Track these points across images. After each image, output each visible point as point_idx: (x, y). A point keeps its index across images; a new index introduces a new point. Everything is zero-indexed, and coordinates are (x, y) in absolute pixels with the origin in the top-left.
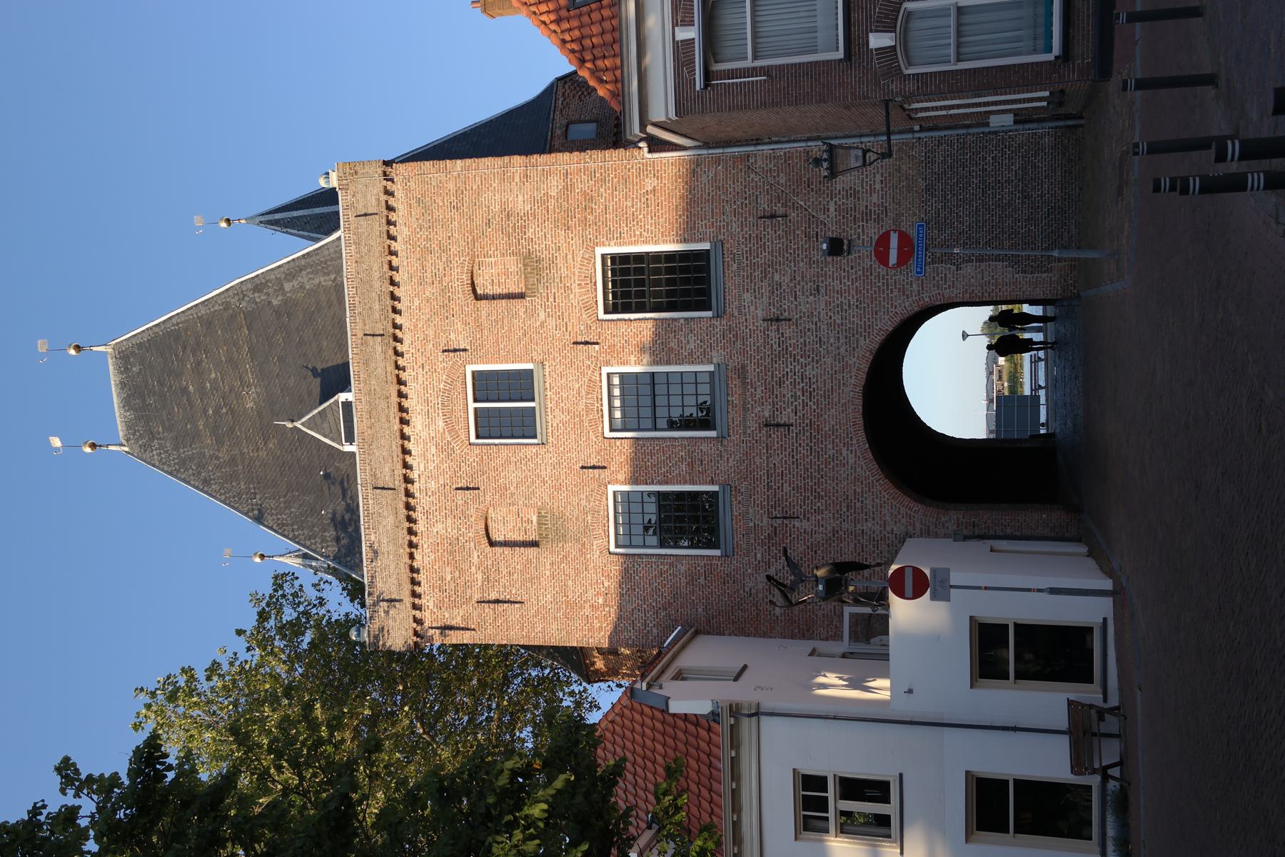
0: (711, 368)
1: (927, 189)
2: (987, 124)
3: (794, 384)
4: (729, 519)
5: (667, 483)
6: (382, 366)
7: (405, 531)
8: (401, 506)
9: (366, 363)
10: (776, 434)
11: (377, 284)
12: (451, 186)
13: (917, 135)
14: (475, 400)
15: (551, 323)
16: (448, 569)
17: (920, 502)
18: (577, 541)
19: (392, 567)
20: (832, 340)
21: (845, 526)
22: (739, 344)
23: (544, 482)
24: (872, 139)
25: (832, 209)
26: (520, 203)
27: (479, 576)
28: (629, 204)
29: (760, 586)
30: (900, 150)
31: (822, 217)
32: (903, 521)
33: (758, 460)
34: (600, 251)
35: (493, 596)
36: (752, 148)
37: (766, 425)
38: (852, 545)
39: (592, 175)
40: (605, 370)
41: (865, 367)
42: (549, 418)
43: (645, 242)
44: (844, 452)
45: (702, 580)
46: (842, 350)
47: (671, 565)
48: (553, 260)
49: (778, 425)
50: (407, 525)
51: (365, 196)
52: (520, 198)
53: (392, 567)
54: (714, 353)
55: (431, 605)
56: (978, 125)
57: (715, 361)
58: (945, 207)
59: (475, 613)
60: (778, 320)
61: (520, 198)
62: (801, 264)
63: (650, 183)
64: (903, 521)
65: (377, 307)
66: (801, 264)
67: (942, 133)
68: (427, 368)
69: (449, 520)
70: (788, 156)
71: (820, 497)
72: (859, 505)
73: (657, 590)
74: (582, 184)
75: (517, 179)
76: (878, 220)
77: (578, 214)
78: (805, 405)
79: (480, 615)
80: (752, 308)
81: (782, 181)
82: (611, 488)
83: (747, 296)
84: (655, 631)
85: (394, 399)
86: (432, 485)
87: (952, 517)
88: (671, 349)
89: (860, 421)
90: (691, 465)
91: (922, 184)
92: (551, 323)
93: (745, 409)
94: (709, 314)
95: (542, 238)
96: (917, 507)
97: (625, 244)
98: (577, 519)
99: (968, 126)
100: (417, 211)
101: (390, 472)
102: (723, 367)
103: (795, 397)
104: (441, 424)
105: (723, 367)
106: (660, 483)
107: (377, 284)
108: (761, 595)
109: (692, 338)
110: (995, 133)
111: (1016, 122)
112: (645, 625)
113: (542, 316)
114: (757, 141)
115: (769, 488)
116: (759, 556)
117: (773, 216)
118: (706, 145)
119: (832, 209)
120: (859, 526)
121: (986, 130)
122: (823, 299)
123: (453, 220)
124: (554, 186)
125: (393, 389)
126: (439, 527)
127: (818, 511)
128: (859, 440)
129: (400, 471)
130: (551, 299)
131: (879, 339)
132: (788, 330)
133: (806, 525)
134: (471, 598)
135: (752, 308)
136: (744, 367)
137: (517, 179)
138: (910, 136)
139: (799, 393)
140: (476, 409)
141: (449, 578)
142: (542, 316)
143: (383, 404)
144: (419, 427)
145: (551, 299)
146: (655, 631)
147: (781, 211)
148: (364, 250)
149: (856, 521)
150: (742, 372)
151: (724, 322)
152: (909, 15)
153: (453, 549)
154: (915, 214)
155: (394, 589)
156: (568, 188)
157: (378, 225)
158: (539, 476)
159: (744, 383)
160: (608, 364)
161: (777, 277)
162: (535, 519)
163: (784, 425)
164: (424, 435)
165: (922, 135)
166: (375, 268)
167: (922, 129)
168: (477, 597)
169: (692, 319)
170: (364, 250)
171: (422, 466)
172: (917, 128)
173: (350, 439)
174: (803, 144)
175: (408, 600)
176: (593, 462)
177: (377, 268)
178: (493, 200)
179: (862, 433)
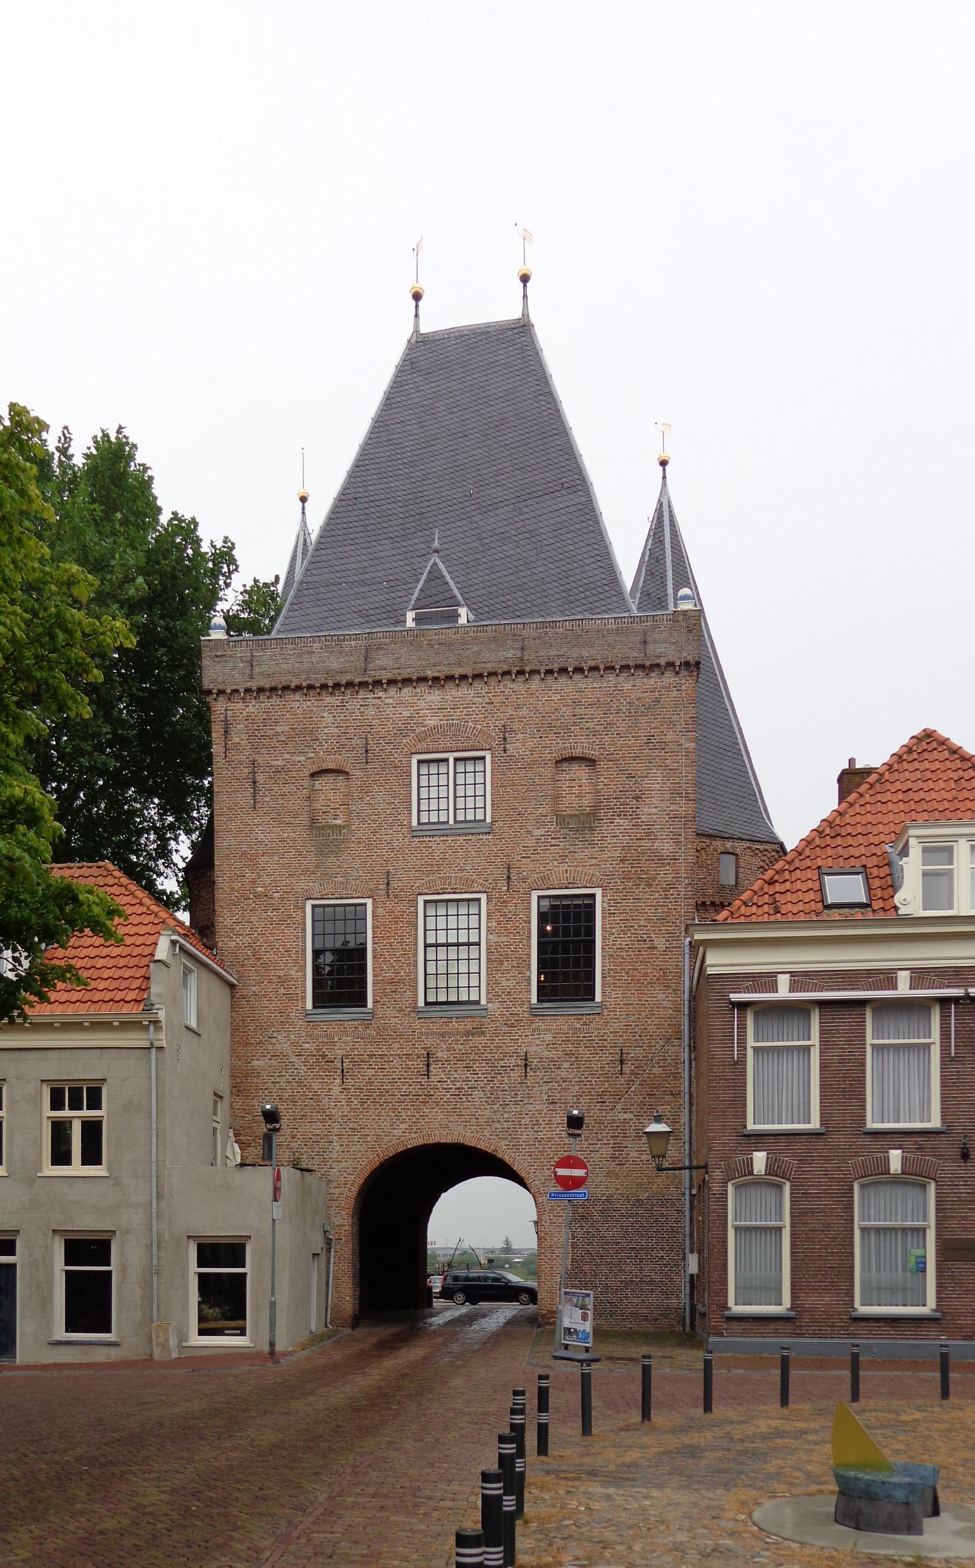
0: (483, 1002)
1: (638, 1201)
2: (692, 1252)
3: (467, 1080)
4: (342, 1017)
5: (374, 957)
6: (492, 658)
7: (323, 681)
8: (349, 677)
9: (495, 640)
10: (420, 1064)
11: (574, 653)
12: (670, 737)
13: (687, 1192)
14: (456, 760)
15: (531, 842)
16: (286, 728)
17: (359, 1193)
18: (317, 867)
19: (285, 666)
20: (506, 1115)
21: (337, 1126)
22: (506, 1029)
23: (374, 833)
24: (687, 1152)
25: (626, 1116)
26: (648, 811)
27: (279, 763)
28: (642, 923)
29: (278, 1047)
30: (676, 1177)
31: (619, 1107)
32: (342, 1179)
33: (396, 1045)
34: (598, 892)
35: (260, 778)
36: (687, 1042)
37: (428, 1054)
38: (318, 1132)
39: (672, 886)
40: (483, 897)
41: (481, 1145)
42: (437, 839)
43: (604, 938)
44: (403, 1126)
45: (282, 991)
46: (497, 1125)
47: (296, 961)
48: (592, 844)
49: (428, 1065)
50: (331, 684)
51: (666, 641)
52: (654, 811)
53: (285, 666)
54: (497, 1005)
55: (251, 709)
56: (692, 1244)
57: (490, 1005)
58: (622, 1216)
59: (243, 758)
60: (526, 1065)
61: (654, 811)
62: (577, 1087)
63: (660, 943)
64: (342, 1179)
65: (553, 653)
66: (577, 1087)
67: (687, 1214)
68: (489, 706)
69: (336, 730)
70: (677, 1076)
71: (362, 1103)
72: (356, 1138)
73: (272, 947)
74: (665, 875)
75: (673, 807)
76: (614, 1158)
77: (636, 871)
78: (448, 1090)
79: (241, 763)
80: (538, 1042)
81: (654, 1070)
82: (369, 902)
83: (549, 1037)
84: (233, 944)
85: (457, 671)
86: (371, 712)
87: (343, 1221)
88: (501, 963)
89: (431, 1141)
90: (391, 982)
91: (644, 1196)
92: (531, 842)
93: (443, 1035)
94: (534, 1000)
95: (615, 831)
96: (355, 1190)
97: (603, 918)
98: (339, 867)
99: (691, 1236)
100: (648, 698)
101: (383, 666)
102: (484, 1013)
103: (454, 1081)
104: (432, 723)
105: (484, 1013)
106: (374, 950)
107: (574, 653)
108: (270, 1047)
109: (512, 983)
110: (684, 1259)
111: (692, 1276)
112: (238, 935)
113: (537, 832)
114: (693, 1048)
115: (370, 1056)
116: (307, 1046)
117: (622, 1062)
118: (693, 998)
119: (626, 1116)
120: (336, 1138)
121: (687, 1251)
122: (544, 1108)
123: (636, 738)
124: (665, 847)
125: (468, 670)
126: (330, 719)
127: (349, 1102)
128: (415, 1140)
129: (385, 676)
130: (553, 842)
131: (507, 1159)
132: (517, 1074)
133: (336, 1090)
134: (258, 753)
135: (538, 1042)
136: (483, 1033)
137: (673, 807)
138: (687, 1186)
139: (458, 1085)
140: (446, 760)
141: (278, 729)
142: (537, 832)
143: (453, 658)
144: (430, 698)
145: (553, 842)
146: (233, 944)
147: (627, 1069)
148: (611, 639)
149: (340, 1136)
150: (479, 1031)
151: (526, 1015)
152: (779, 1187)
153: (306, 734)
154: (617, 1190)
155: (265, 668)
156: (660, 860)
157: (635, 656)
158: (380, 826)
159: (467, 1034)
160: (489, 900)
161: (566, 1065)
162: (339, 822)
163: (428, 1071)
164: (422, 704)
165: (687, 1197)
166: (593, 652)
167: (692, 1196)
168: (259, 759)
169: (529, 984)
170: (611, 639)
171: (391, 701)
172: (694, 1192)
173: (417, 619)
174: (687, 1090)
175: (253, 685)
176: (394, 884)
177: (590, 654)
178: (655, 782)
179: (421, 1142)
